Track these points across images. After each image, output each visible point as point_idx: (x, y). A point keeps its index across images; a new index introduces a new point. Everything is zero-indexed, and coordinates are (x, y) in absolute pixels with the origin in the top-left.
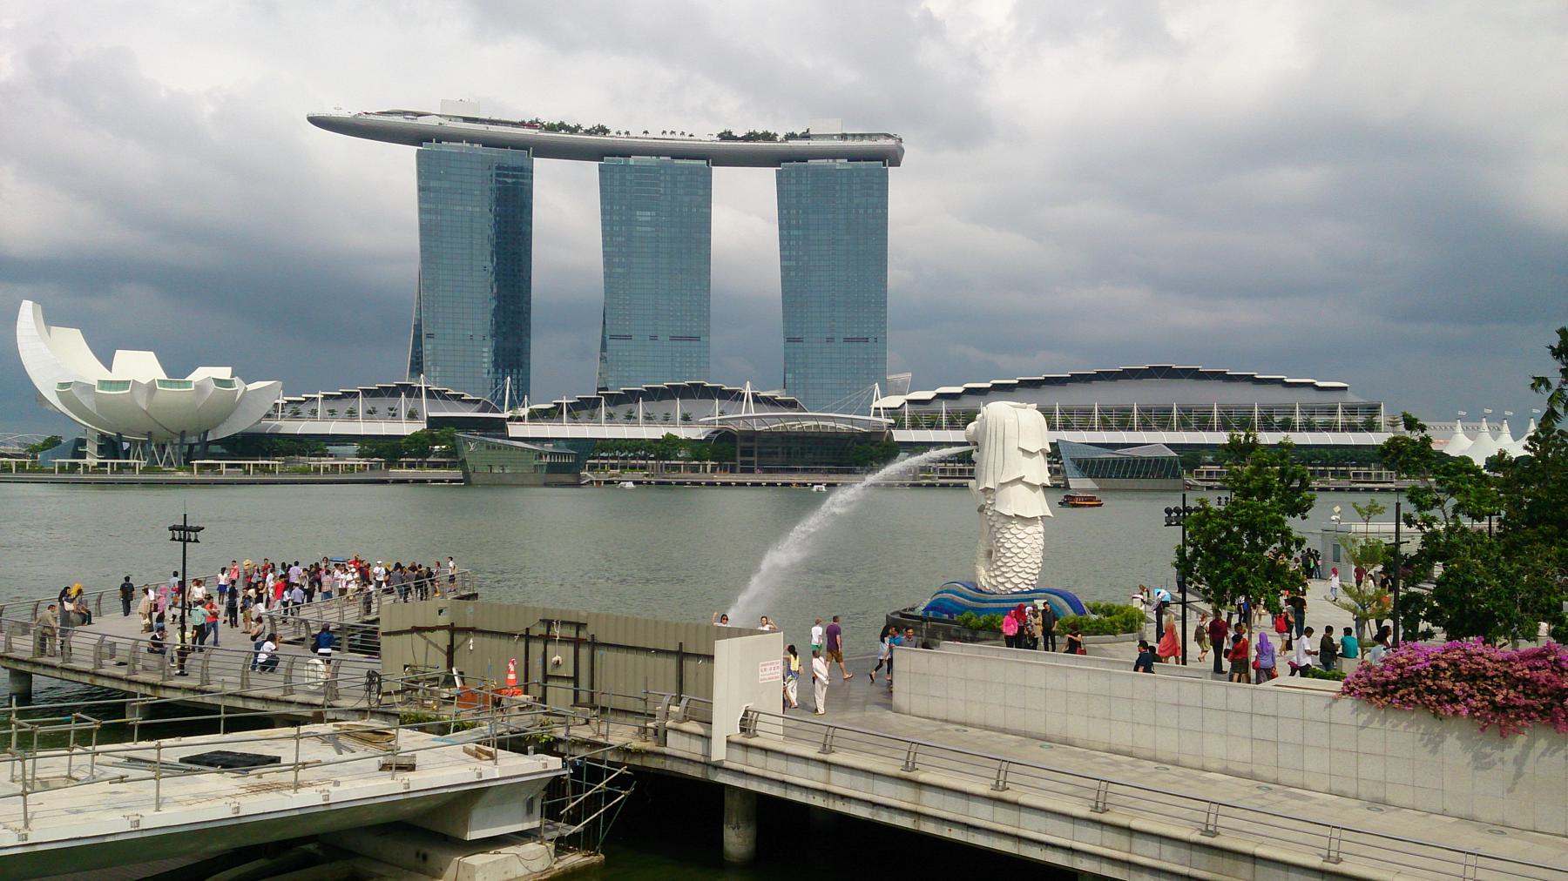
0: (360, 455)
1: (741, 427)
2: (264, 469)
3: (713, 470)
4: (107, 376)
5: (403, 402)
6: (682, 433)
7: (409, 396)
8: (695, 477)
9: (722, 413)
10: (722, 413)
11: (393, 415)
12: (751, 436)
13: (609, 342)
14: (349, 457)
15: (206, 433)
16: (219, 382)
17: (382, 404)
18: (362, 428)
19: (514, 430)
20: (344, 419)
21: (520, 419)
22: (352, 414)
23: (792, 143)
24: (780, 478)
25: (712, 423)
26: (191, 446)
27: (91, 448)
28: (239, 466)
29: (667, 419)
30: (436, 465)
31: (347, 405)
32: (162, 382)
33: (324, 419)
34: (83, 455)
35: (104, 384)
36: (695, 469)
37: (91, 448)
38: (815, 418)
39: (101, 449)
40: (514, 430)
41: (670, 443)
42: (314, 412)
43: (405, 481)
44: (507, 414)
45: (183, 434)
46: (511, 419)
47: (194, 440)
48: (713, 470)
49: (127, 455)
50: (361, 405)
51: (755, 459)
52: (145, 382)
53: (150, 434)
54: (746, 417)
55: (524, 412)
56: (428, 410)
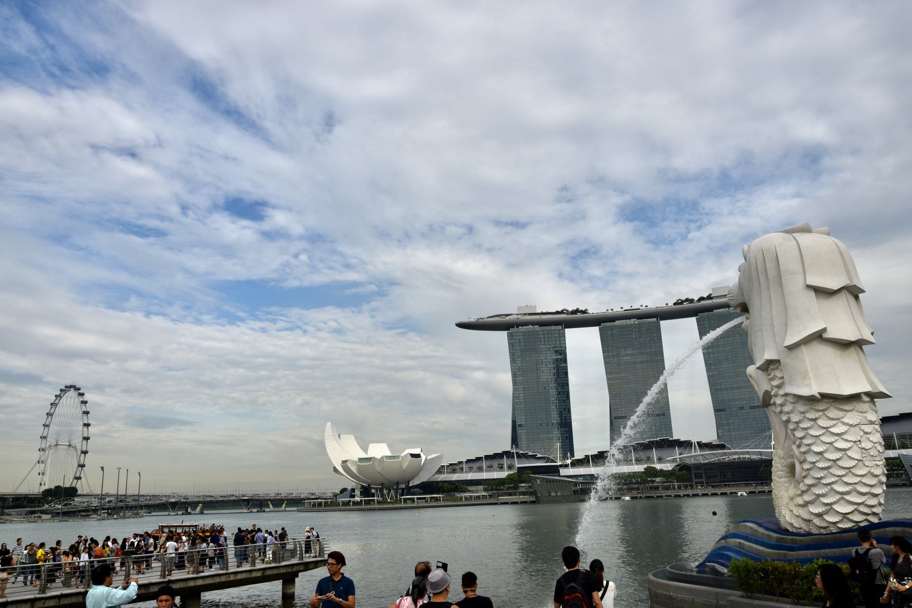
0: (485, 490)
1: (693, 461)
2: (437, 499)
3: (679, 487)
4: (364, 456)
5: (505, 461)
6: (658, 466)
7: (508, 457)
8: (669, 493)
9: (680, 454)
10: (680, 454)
11: (501, 468)
12: (699, 466)
13: (614, 421)
14: (480, 492)
15: (409, 482)
16: (413, 456)
17: (495, 463)
18: (485, 475)
19: (563, 472)
20: (475, 472)
21: (566, 466)
22: (480, 469)
23: (702, 302)
24: (719, 491)
25: (674, 460)
26: (403, 489)
27: (357, 492)
28: (424, 498)
29: (649, 459)
30: (524, 494)
31: (478, 464)
32: (387, 457)
33: (466, 472)
34: (354, 496)
35: (361, 460)
36: (667, 488)
37: (357, 492)
38: (736, 453)
39: (362, 493)
40: (563, 472)
41: (651, 472)
42: (462, 469)
43: (506, 503)
44: (559, 463)
45: (398, 484)
46: (561, 466)
47: (403, 486)
48: (679, 487)
49: (373, 495)
50: (484, 464)
51: (704, 480)
52: (379, 457)
53: (382, 484)
54: (695, 456)
55: (569, 462)
56: (518, 464)
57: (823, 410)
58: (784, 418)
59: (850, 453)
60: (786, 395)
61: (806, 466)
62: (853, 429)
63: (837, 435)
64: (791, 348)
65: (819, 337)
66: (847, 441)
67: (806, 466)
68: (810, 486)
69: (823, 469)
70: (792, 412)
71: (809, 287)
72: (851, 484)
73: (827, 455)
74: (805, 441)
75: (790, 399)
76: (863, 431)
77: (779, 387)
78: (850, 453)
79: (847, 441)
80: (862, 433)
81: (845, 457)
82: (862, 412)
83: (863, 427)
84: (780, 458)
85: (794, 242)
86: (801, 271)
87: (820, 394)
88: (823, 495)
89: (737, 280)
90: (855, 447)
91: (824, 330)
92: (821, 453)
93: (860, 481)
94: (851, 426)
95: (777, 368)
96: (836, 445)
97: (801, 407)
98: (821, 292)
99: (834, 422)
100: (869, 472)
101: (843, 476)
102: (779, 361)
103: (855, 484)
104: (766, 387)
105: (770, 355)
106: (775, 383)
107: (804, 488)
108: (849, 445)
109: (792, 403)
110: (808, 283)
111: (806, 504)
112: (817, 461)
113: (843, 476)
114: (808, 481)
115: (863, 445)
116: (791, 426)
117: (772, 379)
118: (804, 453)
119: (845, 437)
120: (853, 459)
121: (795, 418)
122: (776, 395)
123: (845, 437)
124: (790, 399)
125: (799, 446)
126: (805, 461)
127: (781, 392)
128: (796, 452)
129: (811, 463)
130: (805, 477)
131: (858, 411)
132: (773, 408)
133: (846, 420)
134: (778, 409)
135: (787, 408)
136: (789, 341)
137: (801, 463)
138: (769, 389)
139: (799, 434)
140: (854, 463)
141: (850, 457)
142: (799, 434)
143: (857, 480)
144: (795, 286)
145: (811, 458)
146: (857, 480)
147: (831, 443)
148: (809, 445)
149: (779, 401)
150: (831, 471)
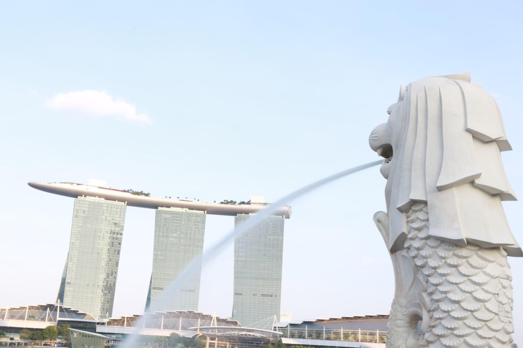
57: (466, 257)
58: (419, 263)
59: (488, 305)
60: (429, 237)
61: (437, 315)
62: (493, 280)
63: (478, 284)
64: (440, 189)
65: (471, 182)
66: (487, 292)
67: (437, 315)
68: (440, 336)
69: (457, 319)
70: (430, 257)
71: (468, 131)
72: (485, 338)
73: (464, 305)
74: (440, 288)
75: (431, 243)
76: (501, 284)
77: (419, 229)
78: (488, 305)
79: (487, 292)
80: (500, 287)
81: (483, 308)
82: (501, 265)
83: (502, 280)
84: (401, 306)
85: (458, 87)
86: (462, 115)
87: (467, 239)
89: (387, 122)
90: (493, 301)
91: (478, 176)
92: (458, 302)
93: (494, 337)
94: (493, 277)
95: (421, 210)
96: (475, 294)
97: (442, 253)
98: (479, 138)
99: (477, 271)
100: (503, 328)
101: (479, 328)
102: (425, 203)
103: (490, 338)
104: (405, 230)
105: (417, 195)
106: (415, 225)
107: (431, 339)
108: (489, 296)
110: (470, 127)
112: (453, 310)
113: (479, 328)
114: (438, 331)
115: (501, 299)
116: (426, 272)
117: (412, 221)
118: (438, 301)
119: (485, 287)
120: (491, 311)
121: (432, 263)
122: (412, 239)
123: (485, 287)
125: (431, 294)
126: (437, 309)
127: (422, 235)
128: (427, 299)
129: (445, 312)
130: (433, 327)
131: (498, 264)
132: (404, 253)
133: (488, 270)
134: (413, 253)
135: (423, 253)
136: (440, 184)
137: (429, 311)
138: (406, 232)
139: (433, 280)
140: (491, 316)
141: (488, 309)
142: (433, 280)
143: (491, 334)
144: (454, 128)
145: (444, 306)
146: (491, 334)
147: (470, 293)
148: (445, 292)
149: (416, 244)
150: (467, 322)
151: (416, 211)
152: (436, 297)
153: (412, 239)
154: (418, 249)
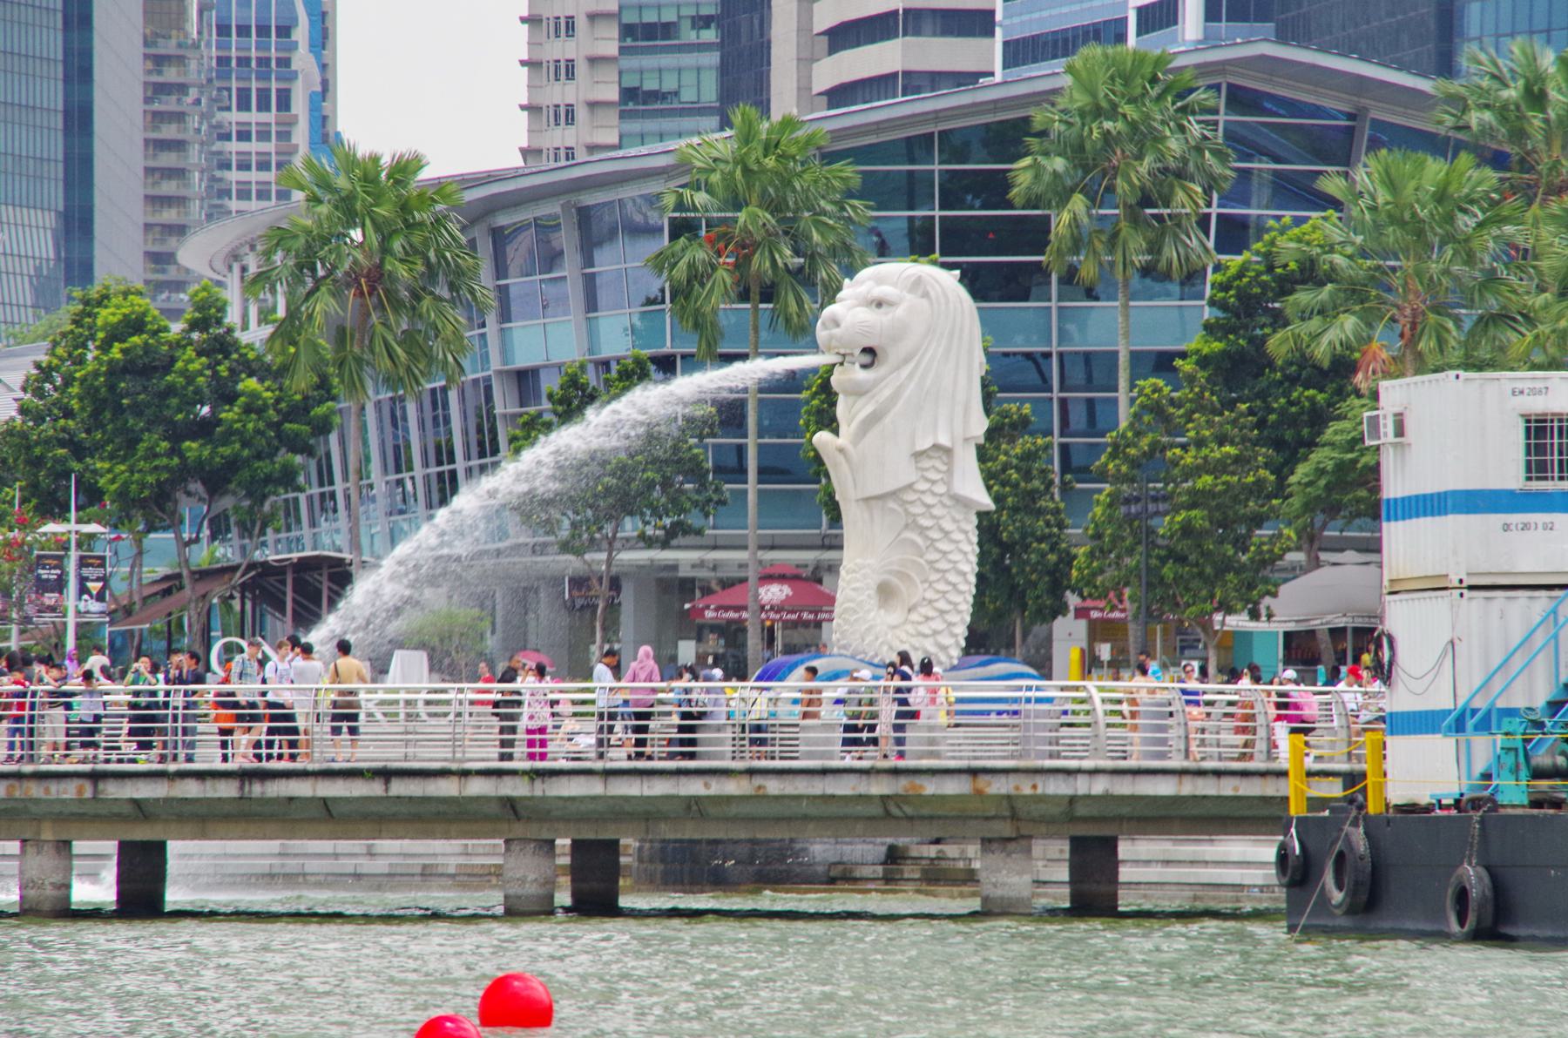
68: (942, 612)
77: (934, 482)
88: (954, 624)
92: (964, 574)
102: (948, 451)
105: (944, 440)
107: (931, 613)
109: (944, 506)
111: (935, 633)
114: (942, 605)
118: (945, 571)
124: (948, 502)
129: (949, 583)
134: (917, 509)
145: (952, 577)
149: (929, 500)
151: (930, 458)
152: (943, 565)
153: (923, 492)
154: (929, 506)
